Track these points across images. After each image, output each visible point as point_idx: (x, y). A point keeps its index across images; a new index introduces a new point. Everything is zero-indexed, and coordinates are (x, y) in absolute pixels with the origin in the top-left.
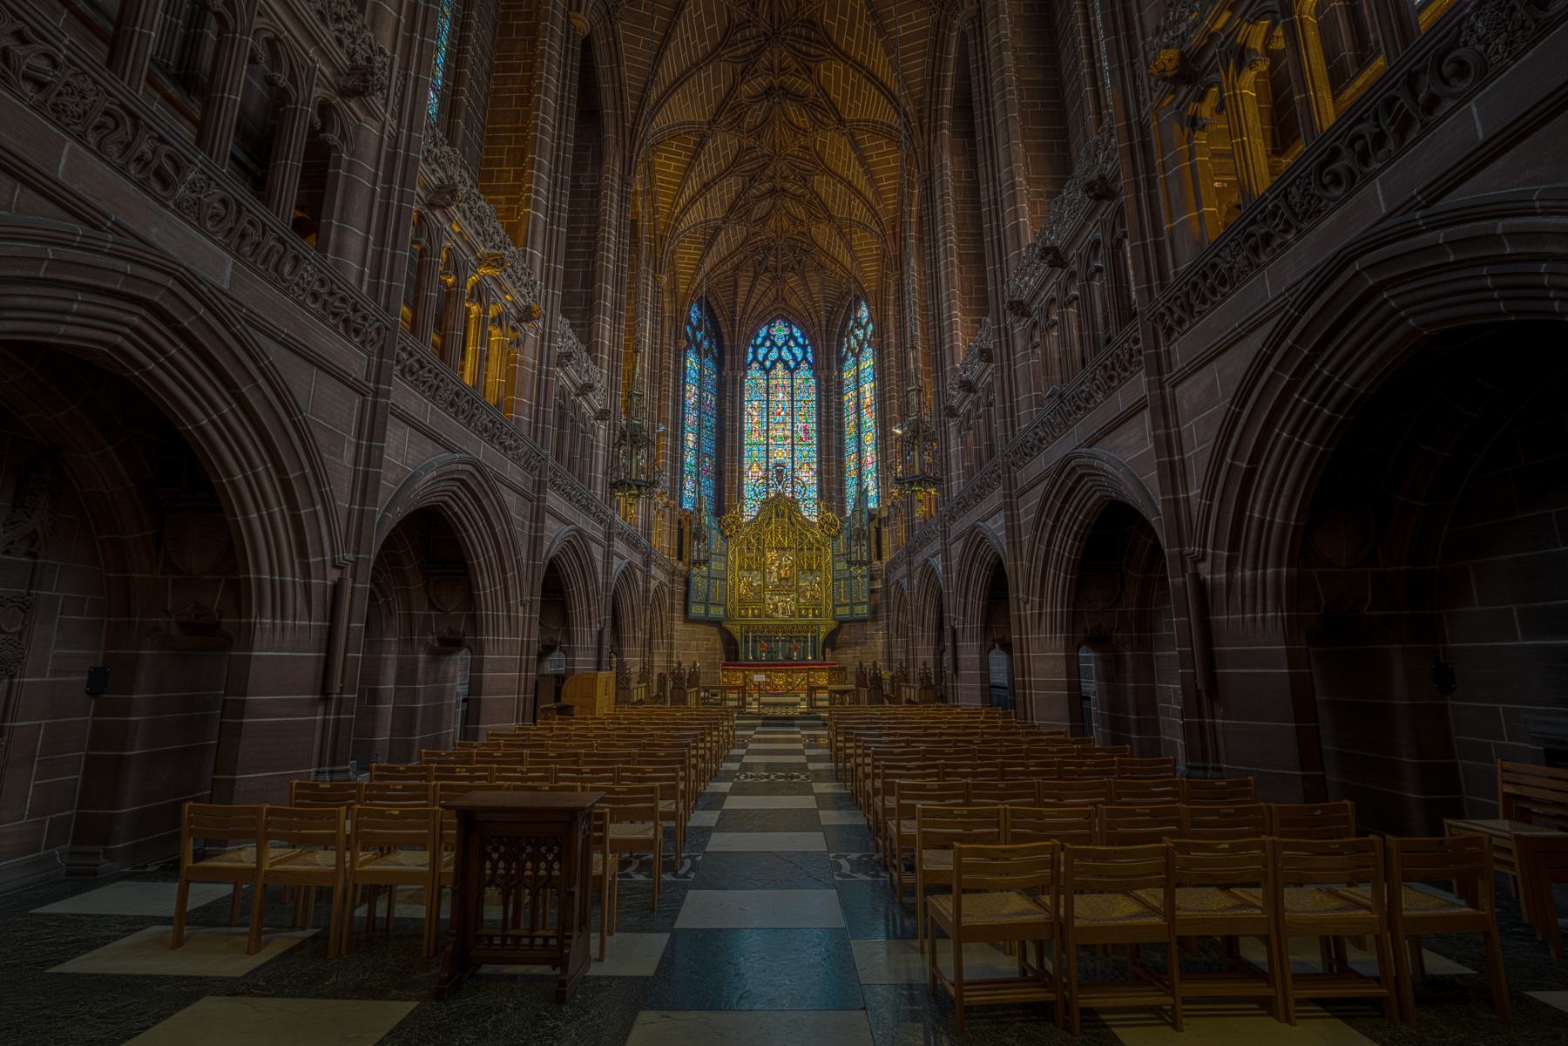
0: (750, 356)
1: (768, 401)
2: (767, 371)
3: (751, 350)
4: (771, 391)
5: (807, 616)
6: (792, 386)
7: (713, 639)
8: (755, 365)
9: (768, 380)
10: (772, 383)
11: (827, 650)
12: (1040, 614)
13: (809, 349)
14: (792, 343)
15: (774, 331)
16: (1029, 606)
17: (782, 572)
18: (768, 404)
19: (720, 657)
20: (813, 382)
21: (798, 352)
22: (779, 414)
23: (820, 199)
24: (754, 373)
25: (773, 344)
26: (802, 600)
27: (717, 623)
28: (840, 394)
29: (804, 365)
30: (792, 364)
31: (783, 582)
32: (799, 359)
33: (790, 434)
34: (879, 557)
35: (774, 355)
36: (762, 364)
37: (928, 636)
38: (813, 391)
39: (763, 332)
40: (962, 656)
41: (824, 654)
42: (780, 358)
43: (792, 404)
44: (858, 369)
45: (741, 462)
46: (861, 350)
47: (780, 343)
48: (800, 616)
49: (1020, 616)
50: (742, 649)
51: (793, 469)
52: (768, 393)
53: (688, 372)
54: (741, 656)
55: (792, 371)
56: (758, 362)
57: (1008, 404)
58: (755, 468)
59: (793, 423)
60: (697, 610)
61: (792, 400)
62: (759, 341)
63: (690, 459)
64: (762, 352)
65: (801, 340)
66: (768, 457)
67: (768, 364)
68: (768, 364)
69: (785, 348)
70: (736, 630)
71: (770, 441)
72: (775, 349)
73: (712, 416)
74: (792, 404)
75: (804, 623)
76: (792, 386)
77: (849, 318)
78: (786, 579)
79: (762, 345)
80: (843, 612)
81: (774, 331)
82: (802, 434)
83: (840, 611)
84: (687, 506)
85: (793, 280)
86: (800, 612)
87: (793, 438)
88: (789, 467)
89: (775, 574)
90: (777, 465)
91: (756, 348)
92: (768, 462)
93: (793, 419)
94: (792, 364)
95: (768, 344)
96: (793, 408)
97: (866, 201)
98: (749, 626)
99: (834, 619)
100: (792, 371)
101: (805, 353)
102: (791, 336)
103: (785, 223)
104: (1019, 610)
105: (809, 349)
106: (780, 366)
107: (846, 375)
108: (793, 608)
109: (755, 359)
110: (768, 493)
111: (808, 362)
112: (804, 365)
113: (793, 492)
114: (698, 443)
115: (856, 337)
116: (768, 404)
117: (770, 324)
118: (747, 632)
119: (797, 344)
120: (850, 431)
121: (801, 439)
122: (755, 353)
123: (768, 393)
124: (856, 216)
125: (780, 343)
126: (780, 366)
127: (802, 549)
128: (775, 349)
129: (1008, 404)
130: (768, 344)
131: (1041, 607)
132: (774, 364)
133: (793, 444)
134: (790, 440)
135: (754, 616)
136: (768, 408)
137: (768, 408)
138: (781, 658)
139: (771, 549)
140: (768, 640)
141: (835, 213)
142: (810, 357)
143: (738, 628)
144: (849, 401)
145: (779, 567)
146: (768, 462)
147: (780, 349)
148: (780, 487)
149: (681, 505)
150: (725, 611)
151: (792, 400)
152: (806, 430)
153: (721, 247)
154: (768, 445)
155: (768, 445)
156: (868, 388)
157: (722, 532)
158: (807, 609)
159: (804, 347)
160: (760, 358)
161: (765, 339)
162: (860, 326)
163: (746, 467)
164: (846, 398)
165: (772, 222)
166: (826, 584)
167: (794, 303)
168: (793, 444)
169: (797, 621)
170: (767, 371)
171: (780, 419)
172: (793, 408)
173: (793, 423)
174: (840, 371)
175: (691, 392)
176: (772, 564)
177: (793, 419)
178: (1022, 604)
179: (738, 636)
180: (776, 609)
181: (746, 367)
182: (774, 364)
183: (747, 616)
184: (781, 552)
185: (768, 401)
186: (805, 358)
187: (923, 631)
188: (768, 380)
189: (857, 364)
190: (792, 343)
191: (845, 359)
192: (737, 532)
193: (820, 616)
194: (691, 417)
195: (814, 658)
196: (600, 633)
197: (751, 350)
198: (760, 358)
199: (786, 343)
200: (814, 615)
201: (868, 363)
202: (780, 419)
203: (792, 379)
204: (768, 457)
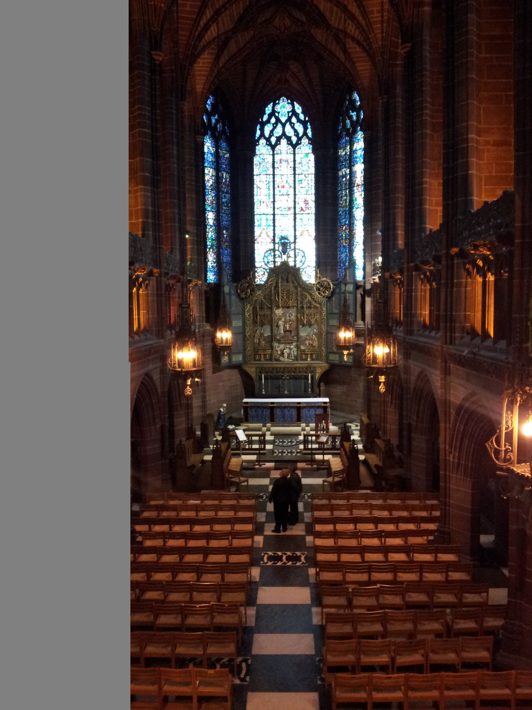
0: (258, 133)
1: (274, 175)
2: (273, 147)
3: (258, 127)
4: (276, 166)
5: (306, 360)
6: (295, 161)
8: (263, 141)
9: (273, 155)
10: (277, 158)
11: (322, 384)
12: (458, 464)
13: (309, 126)
14: (294, 120)
15: (278, 108)
16: (452, 456)
17: (288, 326)
18: (274, 178)
19: (240, 390)
20: (312, 157)
21: (300, 128)
22: (283, 187)
23: (319, 11)
24: (262, 148)
25: (278, 120)
26: (303, 348)
27: (238, 367)
28: (336, 169)
29: (305, 141)
30: (294, 139)
31: (288, 334)
32: (300, 135)
33: (293, 206)
34: (363, 319)
35: (279, 131)
36: (268, 140)
37: (395, 403)
38: (312, 164)
39: (269, 110)
40: (415, 443)
41: (319, 386)
42: (284, 134)
43: (295, 177)
44: (351, 148)
45: (252, 232)
46: (355, 132)
47: (283, 119)
48: (302, 359)
49: (446, 460)
50: (257, 385)
51: (295, 236)
52: (274, 167)
53: (206, 156)
54: (257, 391)
55: (294, 146)
56: (265, 138)
57: (449, 313)
58: (264, 235)
59: (295, 195)
61: (295, 174)
62: (265, 118)
63: (211, 234)
64: (268, 129)
65: (302, 117)
66: (274, 226)
67: (273, 140)
68: (273, 140)
69: (288, 124)
70: (252, 371)
71: (277, 212)
72: (279, 126)
73: (227, 193)
74: (295, 177)
75: (306, 365)
76: (295, 161)
77: (345, 100)
78: (290, 331)
79: (268, 121)
80: (334, 358)
81: (278, 108)
82: (303, 205)
83: (332, 357)
84: (211, 277)
85: (294, 67)
86: (301, 356)
87: (295, 208)
88: (292, 240)
89: (282, 328)
90: (283, 238)
91: (263, 125)
92: (274, 230)
93: (295, 191)
94: (294, 139)
95: (273, 120)
96: (295, 181)
97: (358, 25)
98: (262, 368)
99: (327, 362)
100: (294, 146)
101: (305, 129)
102: (294, 112)
103: (288, 22)
104: (446, 456)
105: (309, 126)
106: (284, 141)
107: (342, 153)
108: (296, 353)
109: (262, 135)
110: (275, 262)
111: (308, 137)
112: (305, 141)
113: (295, 261)
114: (218, 219)
115: (350, 118)
116: (274, 178)
117: (275, 101)
118: (261, 373)
119: (299, 121)
120: (344, 200)
121: (302, 210)
122: (262, 130)
123: (274, 167)
124: (351, 31)
125: (283, 119)
126: (284, 141)
127: (302, 307)
128: (279, 126)
129: (449, 313)
130: (273, 120)
131: (459, 458)
132: (279, 139)
133: (295, 214)
134: (292, 211)
135: (266, 360)
136: (274, 182)
137: (274, 182)
138: (286, 392)
139: (278, 307)
140: (278, 378)
141: (332, 23)
142: (309, 132)
143: (253, 369)
144: (343, 176)
145: (285, 322)
146: (274, 230)
147: (284, 125)
148: (285, 257)
149: (206, 280)
150: (244, 357)
151: (295, 174)
152: (306, 202)
153: (232, 47)
154: (274, 215)
155: (274, 215)
156: (359, 168)
157: (238, 295)
158: (307, 354)
159: (304, 123)
160: (267, 134)
161: (270, 116)
162: (354, 109)
163: (257, 234)
164: (340, 174)
165: (277, 22)
166: (321, 334)
167: (294, 84)
168: (295, 214)
169: (300, 364)
170: (273, 147)
171: (284, 191)
172: (295, 181)
173: (295, 195)
174: (336, 148)
175: (209, 173)
176: (280, 319)
177: (295, 191)
178: (447, 452)
179: (253, 375)
180: (282, 354)
181: (255, 143)
182: (279, 139)
183: (260, 360)
184: (286, 310)
185: (274, 175)
186: (305, 134)
187: (392, 398)
188: (273, 155)
189: (352, 145)
190: (294, 120)
191: (340, 137)
192: (251, 294)
193: (317, 359)
194: (210, 197)
195: (312, 390)
196: (163, 427)
197: (258, 127)
198: (267, 134)
199: (289, 119)
200: (312, 359)
201: (359, 145)
202: (284, 191)
203: (294, 154)
204: (274, 226)
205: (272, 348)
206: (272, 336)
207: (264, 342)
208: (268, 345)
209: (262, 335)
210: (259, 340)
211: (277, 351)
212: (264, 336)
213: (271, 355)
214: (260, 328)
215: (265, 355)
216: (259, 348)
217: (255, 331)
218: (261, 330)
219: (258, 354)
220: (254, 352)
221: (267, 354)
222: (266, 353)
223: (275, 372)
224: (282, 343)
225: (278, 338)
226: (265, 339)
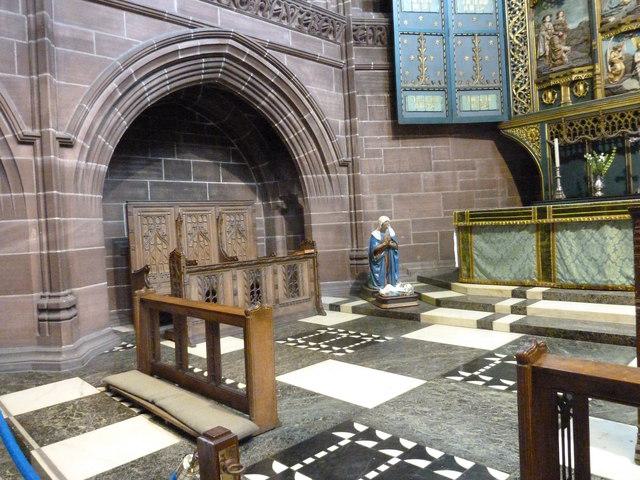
7: (483, 157)
60: (419, 105)
150: (506, 101)
179: (535, 152)
205: (592, 54)
206: (591, 24)
207: (567, 48)
208: (580, 55)
209: (560, 27)
210: (552, 44)
211: (612, 64)
212: (565, 31)
213: (591, 82)
214: (554, 11)
215: (573, 84)
216: (554, 69)
217: (540, 22)
218: (558, 14)
219: (549, 88)
220: (538, 83)
221: (578, 81)
222: (574, 77)
223: (602, 127)
224: (630, 33)
225: (612, 19)
226: (570, 37)
